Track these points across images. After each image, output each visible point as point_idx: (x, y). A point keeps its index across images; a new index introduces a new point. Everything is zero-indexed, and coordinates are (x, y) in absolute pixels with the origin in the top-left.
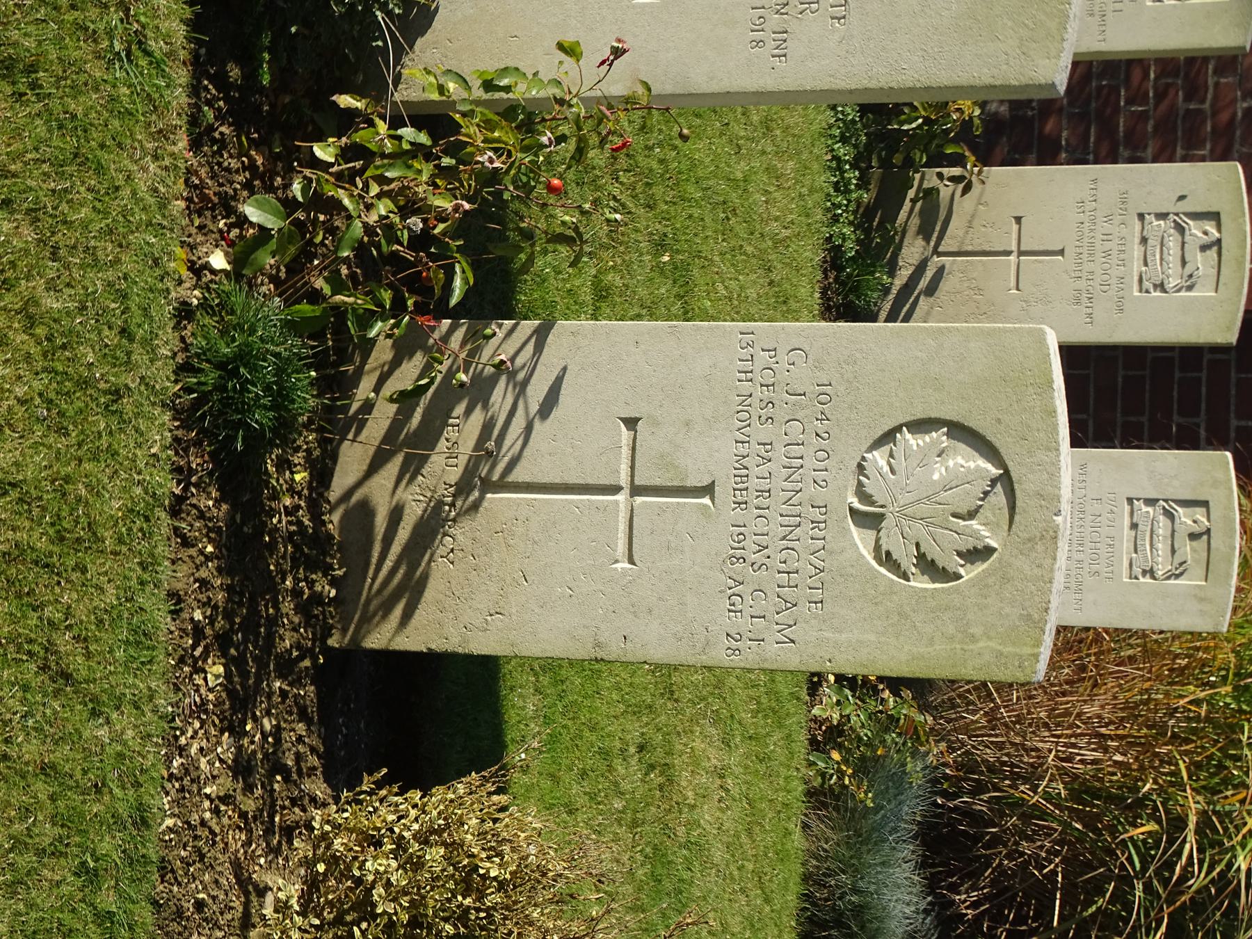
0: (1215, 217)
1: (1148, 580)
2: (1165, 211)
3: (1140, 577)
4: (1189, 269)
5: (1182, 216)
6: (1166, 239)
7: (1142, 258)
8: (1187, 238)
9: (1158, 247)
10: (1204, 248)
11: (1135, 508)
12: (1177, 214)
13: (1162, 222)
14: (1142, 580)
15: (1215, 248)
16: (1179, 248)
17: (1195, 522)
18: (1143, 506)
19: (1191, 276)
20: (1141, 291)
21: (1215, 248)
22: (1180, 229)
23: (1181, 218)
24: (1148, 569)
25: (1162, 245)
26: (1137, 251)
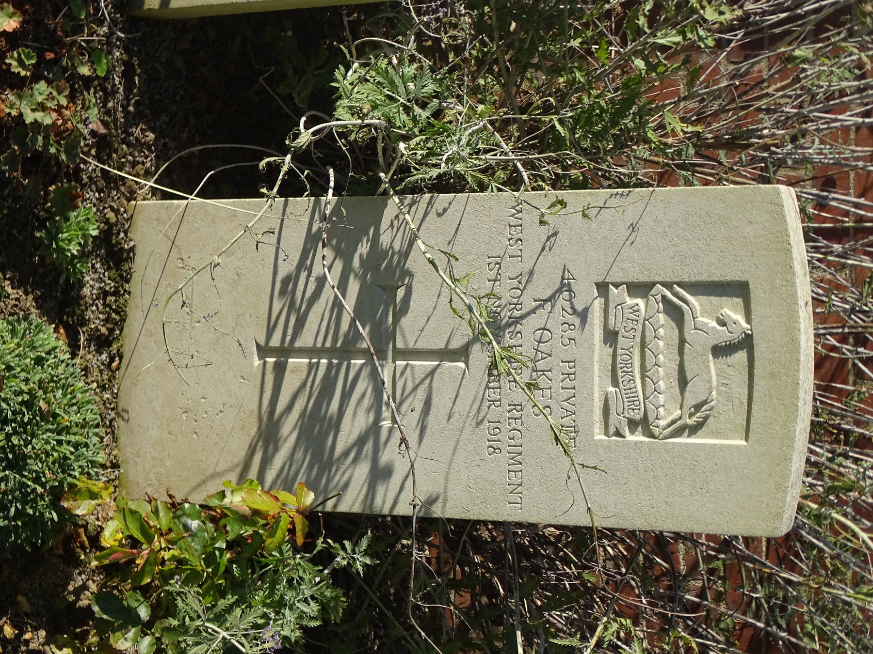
2: (643, 278)
6: (650, 333)
10: (719, 351)
12: (668, 285)
13: (640, 302)
23: (676, 295)
25: (643, 346)
26: (600, 353)
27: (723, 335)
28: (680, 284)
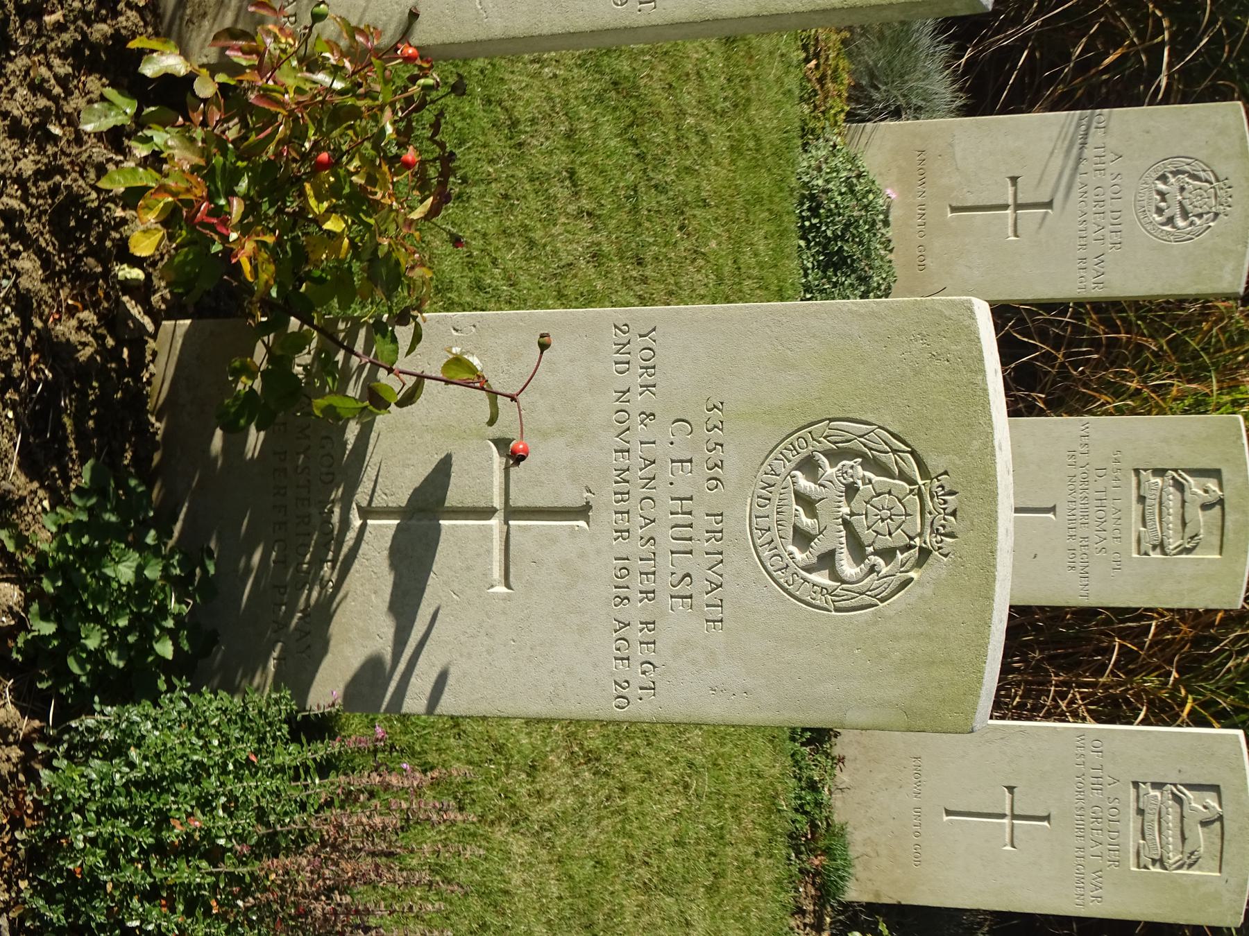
0: (1216, 474)
1: (1157, 869)
3: (1151, 867)
4: (1190, 531)
5: (1180, 472)
7: (1140, 518)
8: (1188, 496)
9: (1157, 506)
10: (1205, 507)
11: (1142, 792)
12: (1176, 470)
13: (1159, 480)
14: (1152, 869)
15: (1218, 507)
16: (1179, 505)
17: (1205, 807)
18: (1150, 790)
19: (1192, 538)
20: (1139, 553)
21: (1218, 507)
22: (1180, 487)
23: (1180, 475)
24: (1157, 857)
25: (1161, 504)
26: (1135, 508)
27: (1209, 498)
28: (1183, 470)
